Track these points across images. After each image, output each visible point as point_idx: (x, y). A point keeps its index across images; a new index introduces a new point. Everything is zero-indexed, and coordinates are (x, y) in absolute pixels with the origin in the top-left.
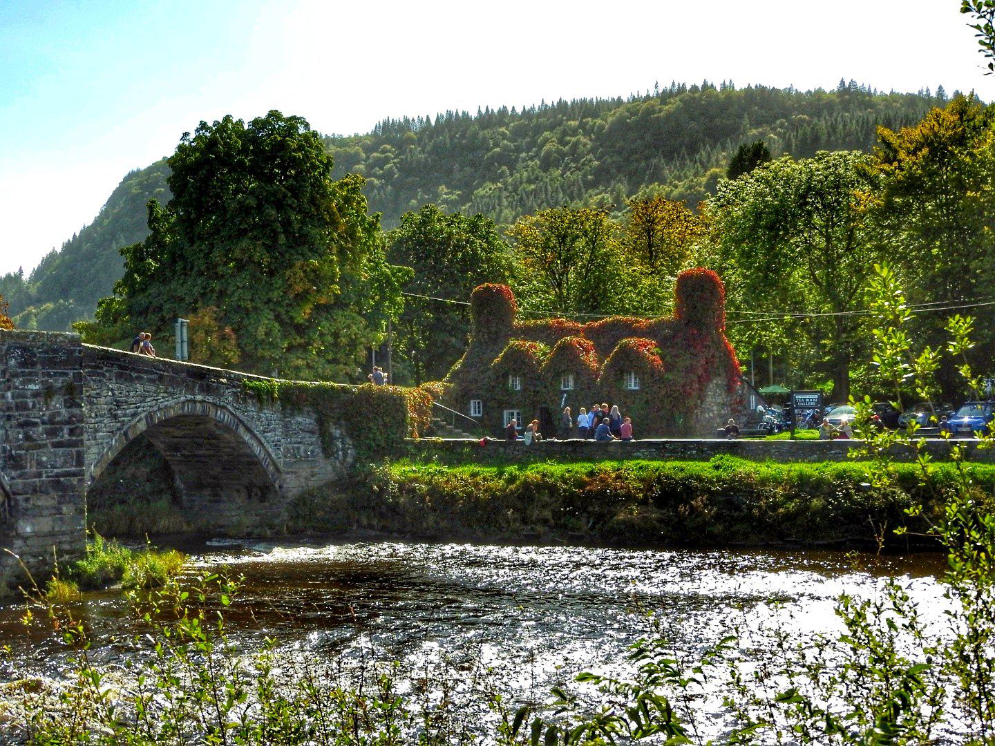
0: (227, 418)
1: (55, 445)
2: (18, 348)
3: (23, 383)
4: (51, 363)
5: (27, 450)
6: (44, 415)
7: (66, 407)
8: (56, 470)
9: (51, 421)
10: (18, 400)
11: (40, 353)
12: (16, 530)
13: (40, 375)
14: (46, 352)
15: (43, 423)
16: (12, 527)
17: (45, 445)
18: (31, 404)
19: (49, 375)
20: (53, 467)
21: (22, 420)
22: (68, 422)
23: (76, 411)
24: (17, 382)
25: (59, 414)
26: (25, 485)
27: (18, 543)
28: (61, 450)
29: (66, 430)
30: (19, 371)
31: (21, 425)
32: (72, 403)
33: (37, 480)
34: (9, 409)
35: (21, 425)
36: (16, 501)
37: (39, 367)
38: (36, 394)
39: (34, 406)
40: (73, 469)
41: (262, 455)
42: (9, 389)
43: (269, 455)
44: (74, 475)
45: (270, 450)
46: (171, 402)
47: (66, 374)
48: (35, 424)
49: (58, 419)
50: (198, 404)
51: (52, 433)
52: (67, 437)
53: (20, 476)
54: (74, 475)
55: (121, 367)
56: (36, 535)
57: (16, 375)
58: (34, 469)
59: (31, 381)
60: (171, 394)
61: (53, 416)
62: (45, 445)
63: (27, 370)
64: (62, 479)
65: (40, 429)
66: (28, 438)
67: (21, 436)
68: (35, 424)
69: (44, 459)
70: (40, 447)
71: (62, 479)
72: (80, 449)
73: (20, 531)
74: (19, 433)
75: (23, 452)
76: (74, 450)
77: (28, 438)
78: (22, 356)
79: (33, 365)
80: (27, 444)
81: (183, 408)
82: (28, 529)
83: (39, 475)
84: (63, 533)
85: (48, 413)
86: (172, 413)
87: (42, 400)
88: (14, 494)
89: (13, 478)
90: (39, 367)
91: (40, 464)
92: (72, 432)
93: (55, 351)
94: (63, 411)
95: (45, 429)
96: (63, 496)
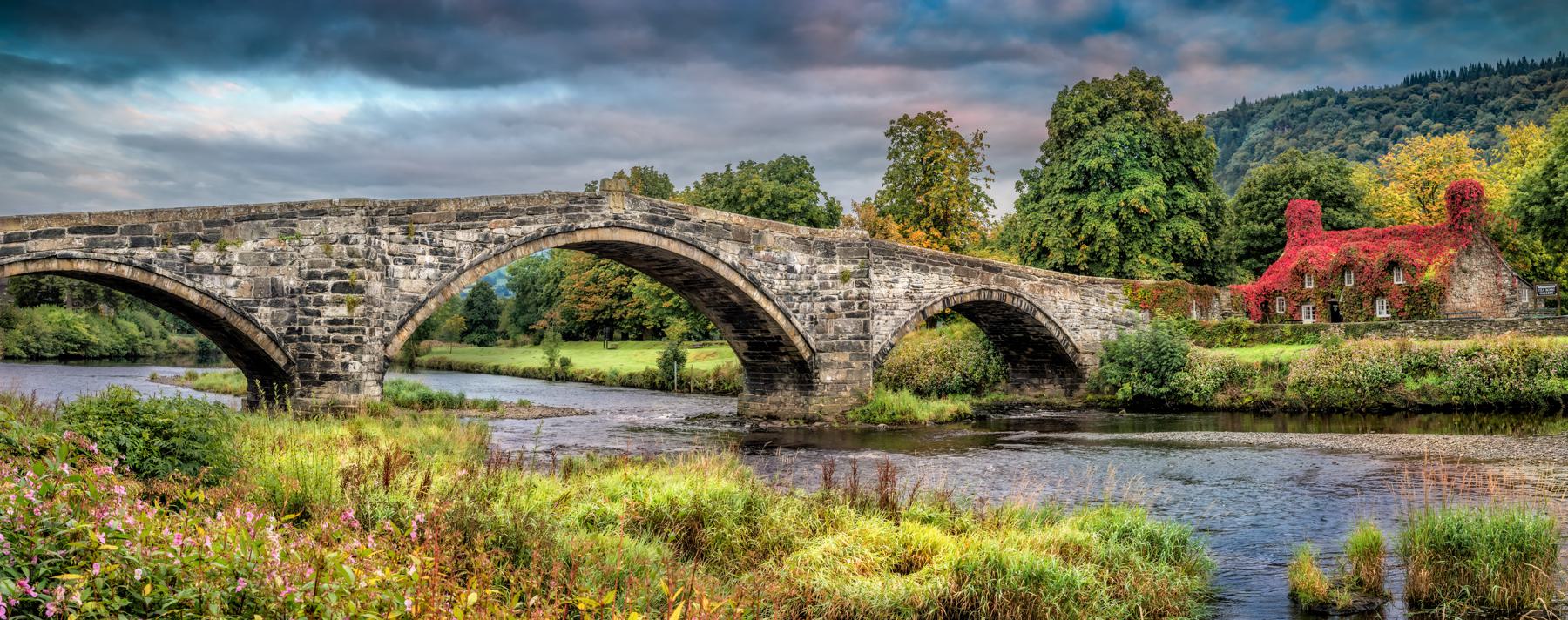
0: (1024, 306)
14: (843, 245)
15: (840, 299)
17: (840, 316)
18: (830, 285)
19: (844, 263)
22: (858, 298)
23: (864, 290)
29: (856, 305)
32: (860, 284)
34: (816, 288)
35: (823, 300)
38: (834, 278)
39: (833, 286)
41: (1061, 337)
42: (815, 272)
43: (1068, 338)
44: (862, 338)
45: (1068, 334)
46: (967, 290)
47: (856, 262)
48: (833, 299)
49: (850, 296)
50: (995, 293)
51: (844, 306)
52: (856, 310)
53: (823, 338)
54: (862, 338)
55: (918, 260)
58: (833, 334)
60: (967, 283)
61: (847, 294)
62: (840, 316)
67: (823, 308)
68: (833, 299)
69: (840, 326)
70: (837, 317)
72: (867, 319)
73: (822, 379)
76: (862, 320)
77: (829, 310)
79: (834, 255)
81: (979, 295)
83: (836, 338)
86: (968, 298)
88: (818, 351)
89: (817, 340)
90: (837, 256)
91: (837, 329)
92: (860, 306)
93: (849, 245)
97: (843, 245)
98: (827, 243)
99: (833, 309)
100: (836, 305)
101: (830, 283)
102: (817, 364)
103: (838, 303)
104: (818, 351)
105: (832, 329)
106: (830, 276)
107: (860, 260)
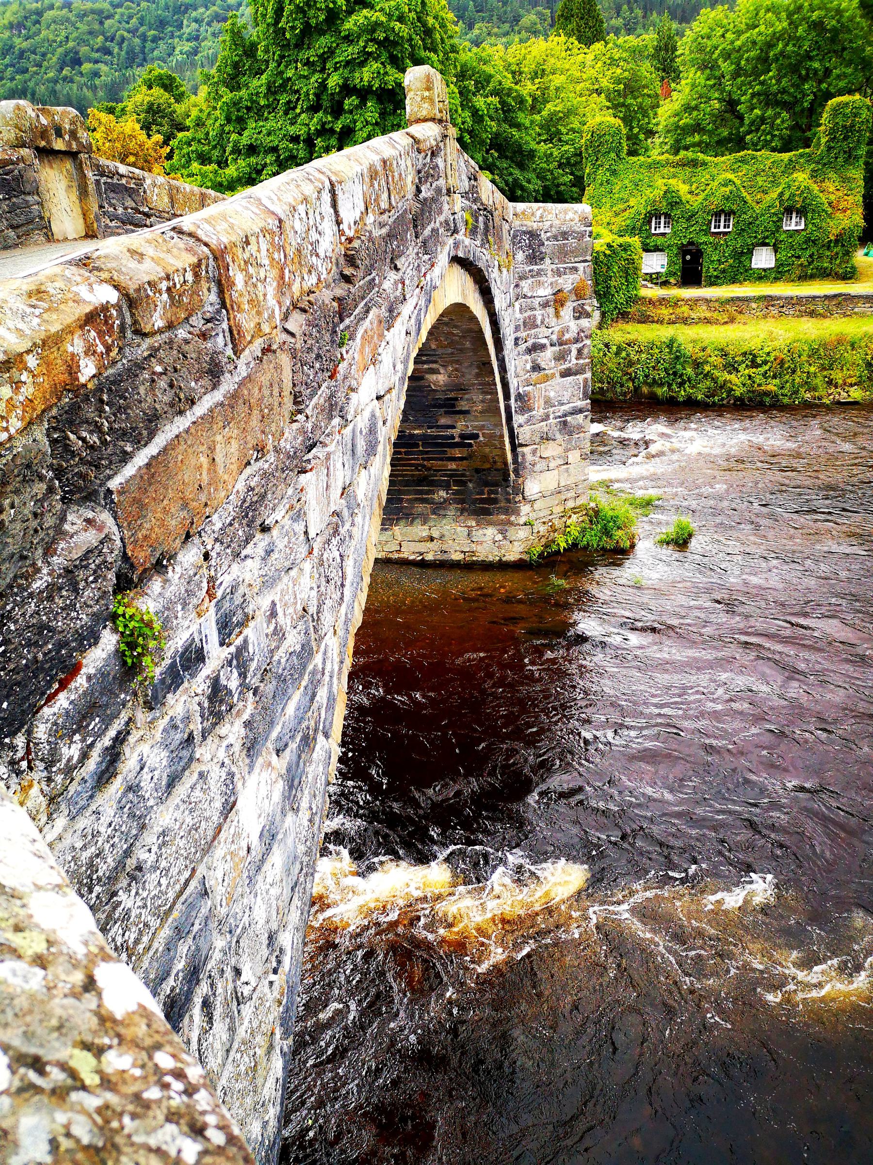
1: (566, 374)
3: (532, 288)
4: (563, 254)
8: (563, 408)
10: (526, 315)
13: (550, 273)
14: (555, 238)
16: (519, 490)
17: (553, 375)
18: (539, 318)
21: (529, 343)
24: (525, 285)
26: (533, 432)
27: (525, 509)
28: (570, 379)
29: (574, 353)
30: (527, 269)
31: (529, 351)
33: (544, 423)
35: (529, 351)
38: (545, 305)
48: (542, 347)
49: (567, 336)
51: (561, 357)
52: (574, 361)
61: (562, 333)
63: (535, 268)
64: (569, 419)
65: (550, 352)
66: (536, 368)
68: (542, 347)
69: (552, 394)
70: (547, 378)
71: (569, 419)
74: (526, 361)
75: (530, 388)
77: (536, 368)
80: (535, 375)
88: (521, 445)
90: (548, 261)
91: (548, 403)
93: (565, 235)
96: (570, 441)
97: (555, 238)
98: (533, 235)
99: (543, 365)
100: (546, 358)
101: (539, 314)
103: (550, 352)
104: (521, 445)
105: (542, 402)
107: (581, 266)
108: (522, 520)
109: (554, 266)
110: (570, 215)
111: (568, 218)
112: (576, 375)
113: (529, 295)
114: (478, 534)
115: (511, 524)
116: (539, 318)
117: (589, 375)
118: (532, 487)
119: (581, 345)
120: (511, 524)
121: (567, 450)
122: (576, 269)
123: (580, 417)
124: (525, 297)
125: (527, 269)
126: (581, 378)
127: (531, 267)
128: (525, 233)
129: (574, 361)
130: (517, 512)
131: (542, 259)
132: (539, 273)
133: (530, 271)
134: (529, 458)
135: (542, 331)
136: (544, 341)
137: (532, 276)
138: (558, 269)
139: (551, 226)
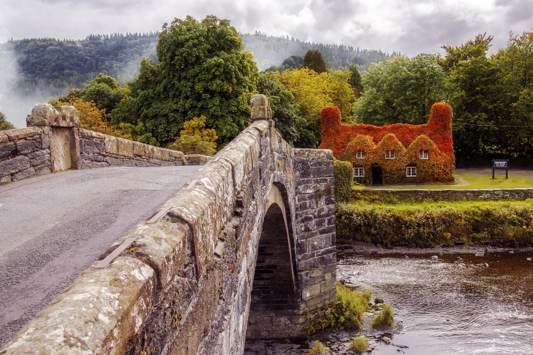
1: (322, 232)
2: (299, 162)
3: (304, 190)
4: (319, 173)
5: (306, 239)
6: (315, 212)
7: (327, 204)
8: (321, 250)
9: (319, 216)
10: (301, 202)
11: (312, 165)
12: (301, 297)
13: (313, 182)
14: (315, 165)
15: (315, 218)
17: (316, 233)
18: (308, 204)
19: (317, 182)
20: (321, 248)
21: (304, 216)
24: (301, 188)
25: (322, 209)
26: (306, 263)
27: (303, 306)
28: (325, 235)
29: (326, 221)
30: (301, 180)
31: (303, 221)
33: (311, 259)
35: (303, 221)
36: (301, 276)
37: (312, 176)
38: (311, 197)
40: (330, 248)
48: (310, 219)
49: (322, 213)
51: (319, 224)
52: (326, 226)
56: (312, 298)
57: (299, 184)
59: (308, 187)
63: (306, 179)
64: (325, 256)
65: (313, 222)
67: (303, 229)
68: (310, 219)
69: (316, 243)
70: (313, 235)
71: (325, 256)
74: (302, 226)
75: (304, 240)
77: (307, 230)
78: (303, 169)
80: (306, 234)
82: (308, 295)
84: (325, 293)
85: (317, 210)
87: (314, 200)
90: (312, 176)
91: (314, 247)
93: (320, 164)
94: (325, 207)
95: (316, 222)
96: (325, 268)
102: (299, 282)
103: (313, 222)
105: (310, 247)
106: (307, 196)
107: (328, 179)
108: (301, 312)
109: (315, 179)
110: (322, 154)
111: (321, 155)
112: (328, 233)
113: (303, 192)
114: (276, 320)
115: (296, 315)
116: (308, 204)
117: (334, 233)
118: (307, 294)
119: (330, 218)
120: (296, 315)
121: (324, 273)
122: (326, 180)
123: (331, 255)
124: (301, 193)
125: (301, 180)
126: (330, 234)
127: (304, 179)
128: (299, 162)
129: (326, 226)
130: (298, 308)
131: (309, 175)
132: (308, 182)
133: (303, 181)
134: (305, 277)
135: (310, 211)
136: (311, 216)
137: (304, 184)
138: (317, 180)
139: (313, 159)
